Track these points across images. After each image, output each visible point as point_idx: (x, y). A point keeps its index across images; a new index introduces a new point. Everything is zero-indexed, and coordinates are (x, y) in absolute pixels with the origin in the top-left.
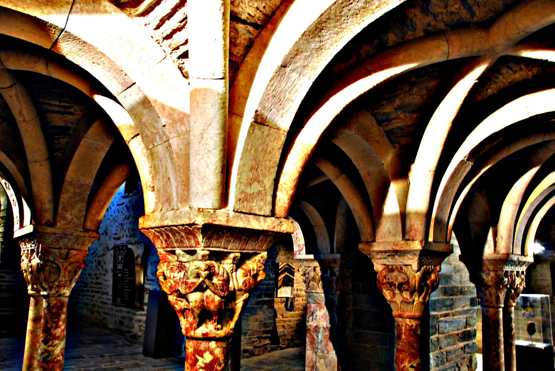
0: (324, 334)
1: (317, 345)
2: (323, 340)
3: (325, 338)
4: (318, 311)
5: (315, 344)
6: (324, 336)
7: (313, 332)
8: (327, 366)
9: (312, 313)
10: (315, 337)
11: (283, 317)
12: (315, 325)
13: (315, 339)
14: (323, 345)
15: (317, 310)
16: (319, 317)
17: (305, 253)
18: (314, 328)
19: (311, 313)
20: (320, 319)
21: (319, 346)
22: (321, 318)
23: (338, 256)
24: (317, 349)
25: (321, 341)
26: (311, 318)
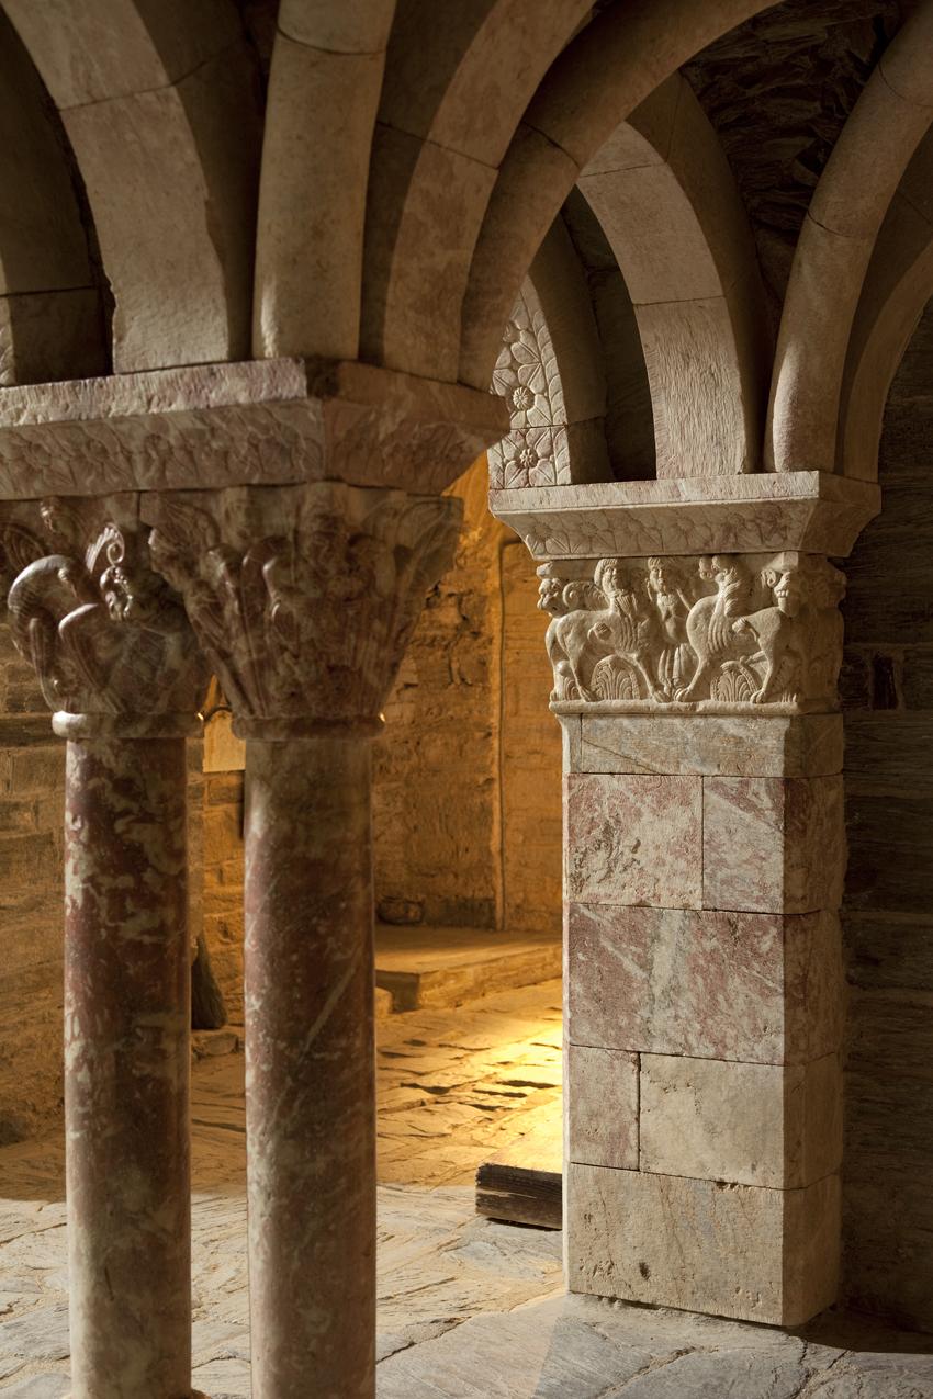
0: (694, 948)
1: (644, 1013)
2: (684, 979)
3: (695, 969)
4: (647, 817)
5: (632, 1010)
8: (711, 1130)
9: (607, 830)
10: (629, 965)
11: (221, 882)
12: (629, 896)
13: (628, 978)
14: (685, 1012)
15: (639, 814)
16: (653, 854)
17: (565, 475)
18: (618, 919)
19: (597, 833)
20: (660, 862)
21: (661, 1019)
22: (669, 859)
23: (804, 485)
24: (647, 1034)
25: (676, 988)
26: (598, 860)
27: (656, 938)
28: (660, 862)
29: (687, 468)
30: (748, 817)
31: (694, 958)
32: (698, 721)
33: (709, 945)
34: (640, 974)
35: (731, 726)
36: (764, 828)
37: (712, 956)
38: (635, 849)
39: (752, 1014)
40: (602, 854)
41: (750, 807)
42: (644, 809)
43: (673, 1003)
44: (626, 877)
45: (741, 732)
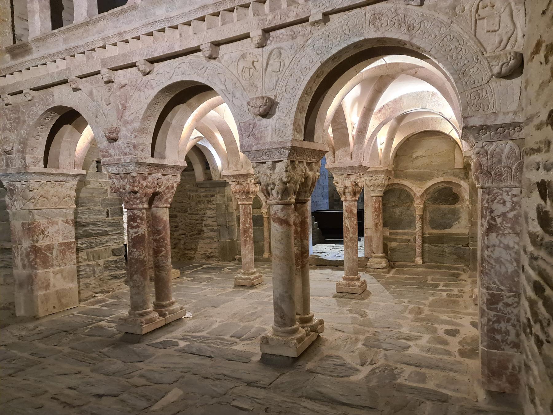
0: (60, 249)
1: (52, 262)
3: (61, 252)
4: (50, 227)
6: (60, 250)
7: (45, 251)
8: (65, 279)
9: (42, 231)
10: (48, 254)
13: (48, 257)
15: (48, 227)
16: (52, 234)
19: (40, 231)
20: (53, 235)
22: (54, 234)
27: (53, 248)
28: (53, 235)
29: (65, 167)
30: (68, 225)
31: (60, 250)
32: (58, 210)
33: (63, 248)
34: (51, 255)
35: (64, 210)
36: (71, 227)
37: (63, 249)
38: (48, 233)
39: (71, 257)
40: (42, 235)
41: (68, 224)
42: (50, 226)
43: (57, 259)
44: (46, 239)
45: (66, 211)
